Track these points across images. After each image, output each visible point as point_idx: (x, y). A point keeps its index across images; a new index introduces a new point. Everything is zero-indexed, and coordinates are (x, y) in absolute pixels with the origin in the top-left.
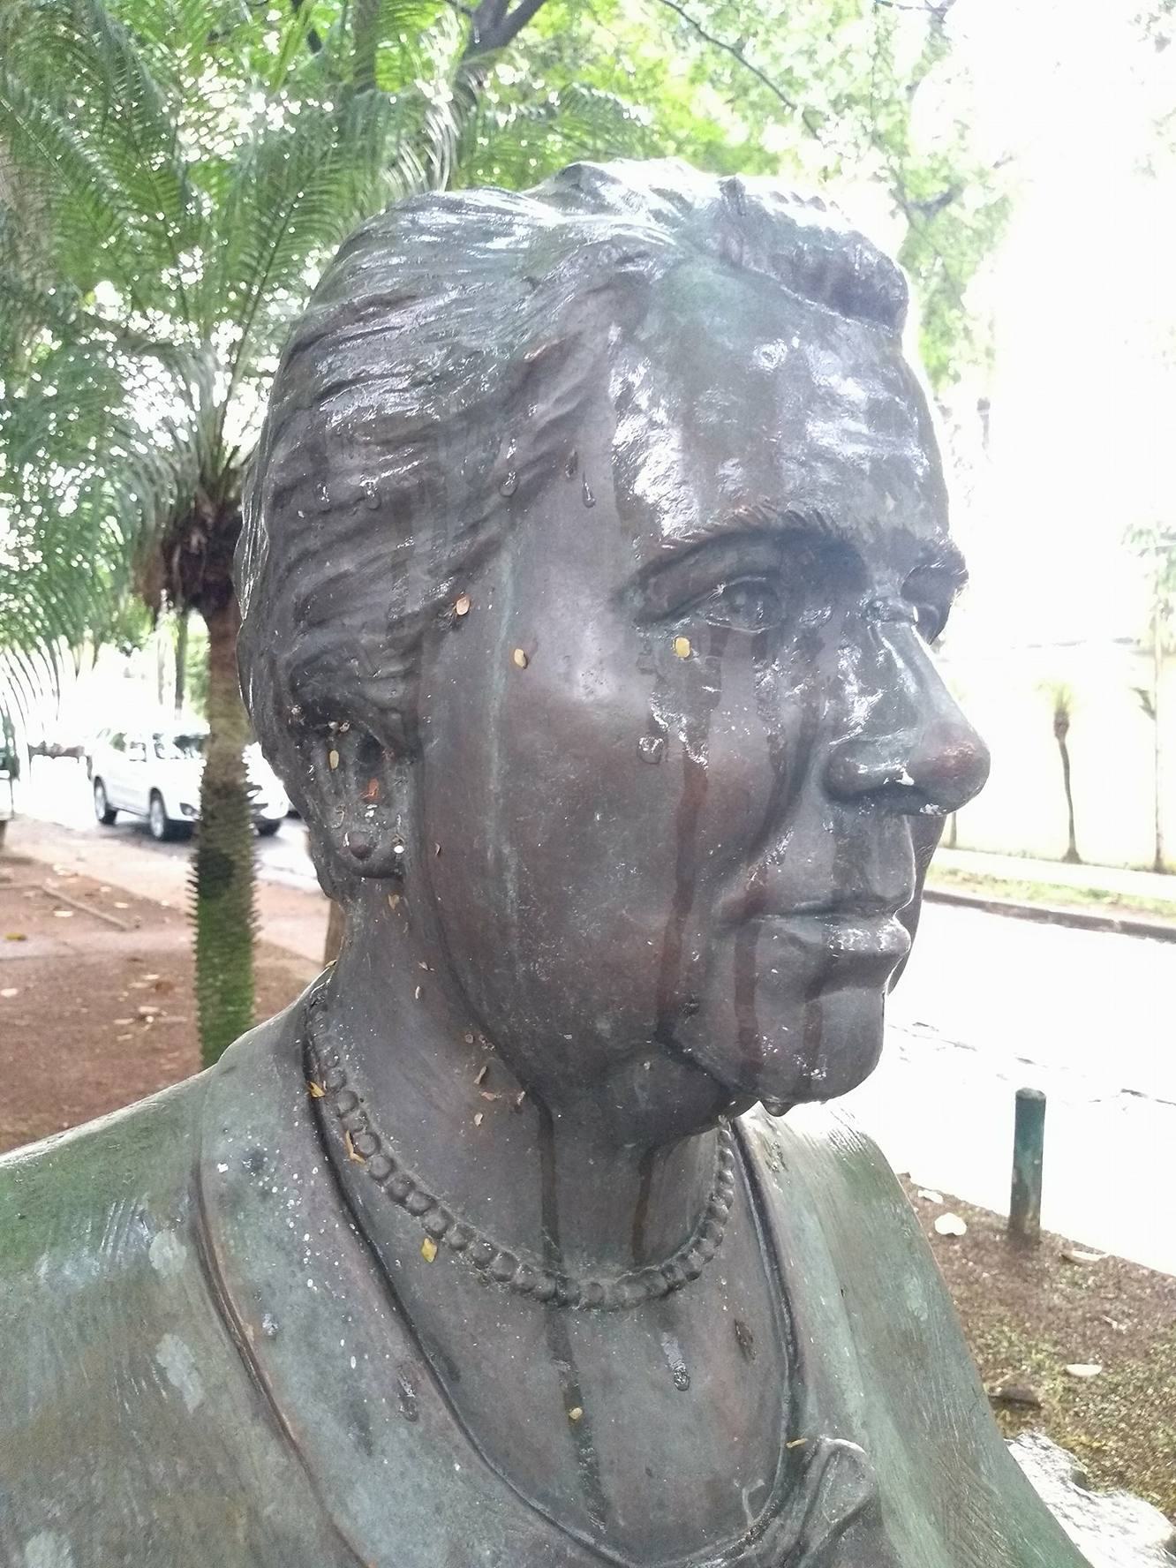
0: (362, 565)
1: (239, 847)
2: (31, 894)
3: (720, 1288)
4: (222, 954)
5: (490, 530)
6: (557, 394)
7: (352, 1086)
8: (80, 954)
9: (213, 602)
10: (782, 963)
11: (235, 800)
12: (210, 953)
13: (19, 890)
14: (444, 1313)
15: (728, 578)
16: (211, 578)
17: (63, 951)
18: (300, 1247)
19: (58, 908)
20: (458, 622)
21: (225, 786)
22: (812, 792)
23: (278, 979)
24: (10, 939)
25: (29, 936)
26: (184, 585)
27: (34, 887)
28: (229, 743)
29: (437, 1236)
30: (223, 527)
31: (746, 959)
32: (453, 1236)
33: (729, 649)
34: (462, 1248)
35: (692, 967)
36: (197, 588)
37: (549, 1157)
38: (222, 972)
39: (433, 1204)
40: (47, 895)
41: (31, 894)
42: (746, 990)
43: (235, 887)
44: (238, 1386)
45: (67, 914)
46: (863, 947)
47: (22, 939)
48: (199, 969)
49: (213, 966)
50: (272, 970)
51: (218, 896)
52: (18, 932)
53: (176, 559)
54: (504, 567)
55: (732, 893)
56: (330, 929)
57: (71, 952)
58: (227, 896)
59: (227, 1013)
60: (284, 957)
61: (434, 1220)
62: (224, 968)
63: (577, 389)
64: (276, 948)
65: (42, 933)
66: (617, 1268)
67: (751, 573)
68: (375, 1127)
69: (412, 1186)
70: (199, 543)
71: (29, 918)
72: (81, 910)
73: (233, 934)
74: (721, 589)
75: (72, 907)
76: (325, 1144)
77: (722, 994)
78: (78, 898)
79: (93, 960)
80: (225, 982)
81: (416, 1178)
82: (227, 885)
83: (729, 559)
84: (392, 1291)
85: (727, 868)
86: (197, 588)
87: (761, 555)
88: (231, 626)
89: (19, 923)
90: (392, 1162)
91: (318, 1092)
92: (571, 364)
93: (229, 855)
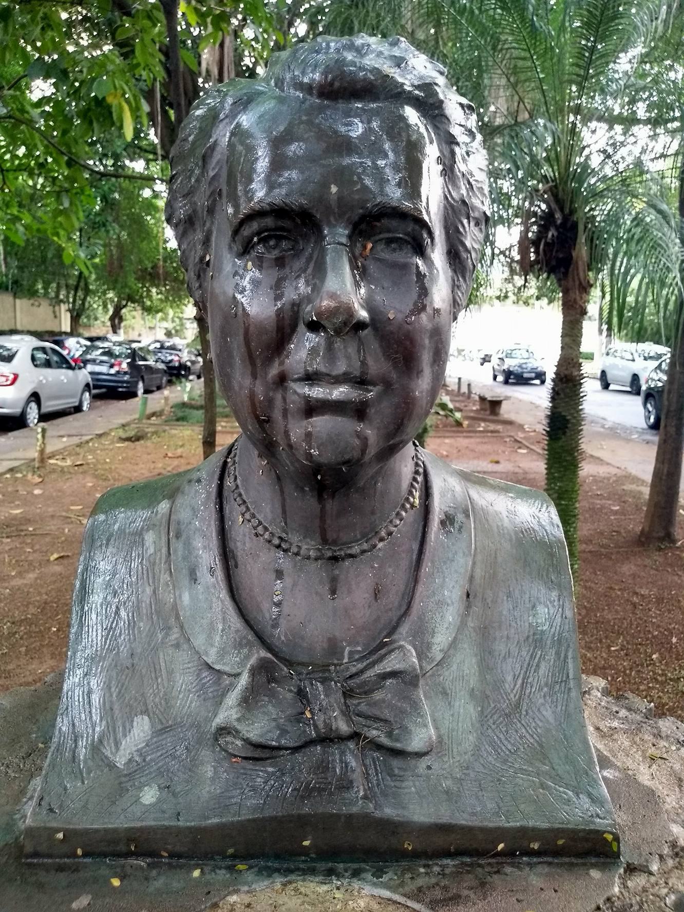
0: (188, 245)
1: (572, 411)
2: (508, 440)
3: (373, 567)
4: (560, 472)
5: (208, 225)
6: (213, 166)
7: (237, 459)
8: (526, 473)
9: (562, 270)
10: (293, 403)
11: (571, 384)
12: (553, 471)
13: (502, 437)
14: (239, 544)
15: (258, 233)
16: (561, 256)
17: (517, 470)
18: (199, 511)
19: (520, 448)
20: (208, 263)
21: (566, 376)
22: (302, 328)
23: (634, 497)
24: (492, 462)
25: (501, 461)
26: (547, 261)
27: (510, 436)
28: (570, 351)
29: (243, 515)
30: (569, 225)
31: (284, 399)
32: (247, 516)
33: (264, 265)
34: (249, 521)
35: (260, 402)
36: (554, 263)
37: (282, 491)
38: (561, 481)
39: (244, 502)
40: (516, 441)
41: (508, 440)
42: (285, 412)
43: (568, 434)
44: (164, 550)
45: (524, 451)
46: (321, 396)
47: (497, 462)
48: (547, 479)
49: (554, 478)
50: (631, 491)
51: (559, 439)
52: (496, 459)
53: (542, 247)
54: (213, 239)
55: (274, 371)
56: (655, 468)
57: (521, 471)
58: (563, 438)
59: (562, 505)
60: (642, 485)
61: (243, 508)
62: (560, 479)
63: (218, 162)
64: (639, 479)
65: (509, 460)
66: (313, 543)
67: (266, 230)
68: (237, 473)
69: (240, 495)
70: (553, 235)
71: (504, 452)
72: (532, 449)
73: (566, 461)
74: (255, 239)
75: (528, 447)
76: (222, 478)
77: (277, 415)
78: (532, 444)
79: (532, 476)
80: (560, 487)
81: (243, 493)
82: (564, 433)
83: (255, 226)
84: (223, 533)
85: (268, 361)
86: (554, 263)
87: (269, 222)
88: (571, 283)
89: (498, 454)
90: (237, 487)
91: (229, 460)
92: (215, 153)
93: (565, 416)
